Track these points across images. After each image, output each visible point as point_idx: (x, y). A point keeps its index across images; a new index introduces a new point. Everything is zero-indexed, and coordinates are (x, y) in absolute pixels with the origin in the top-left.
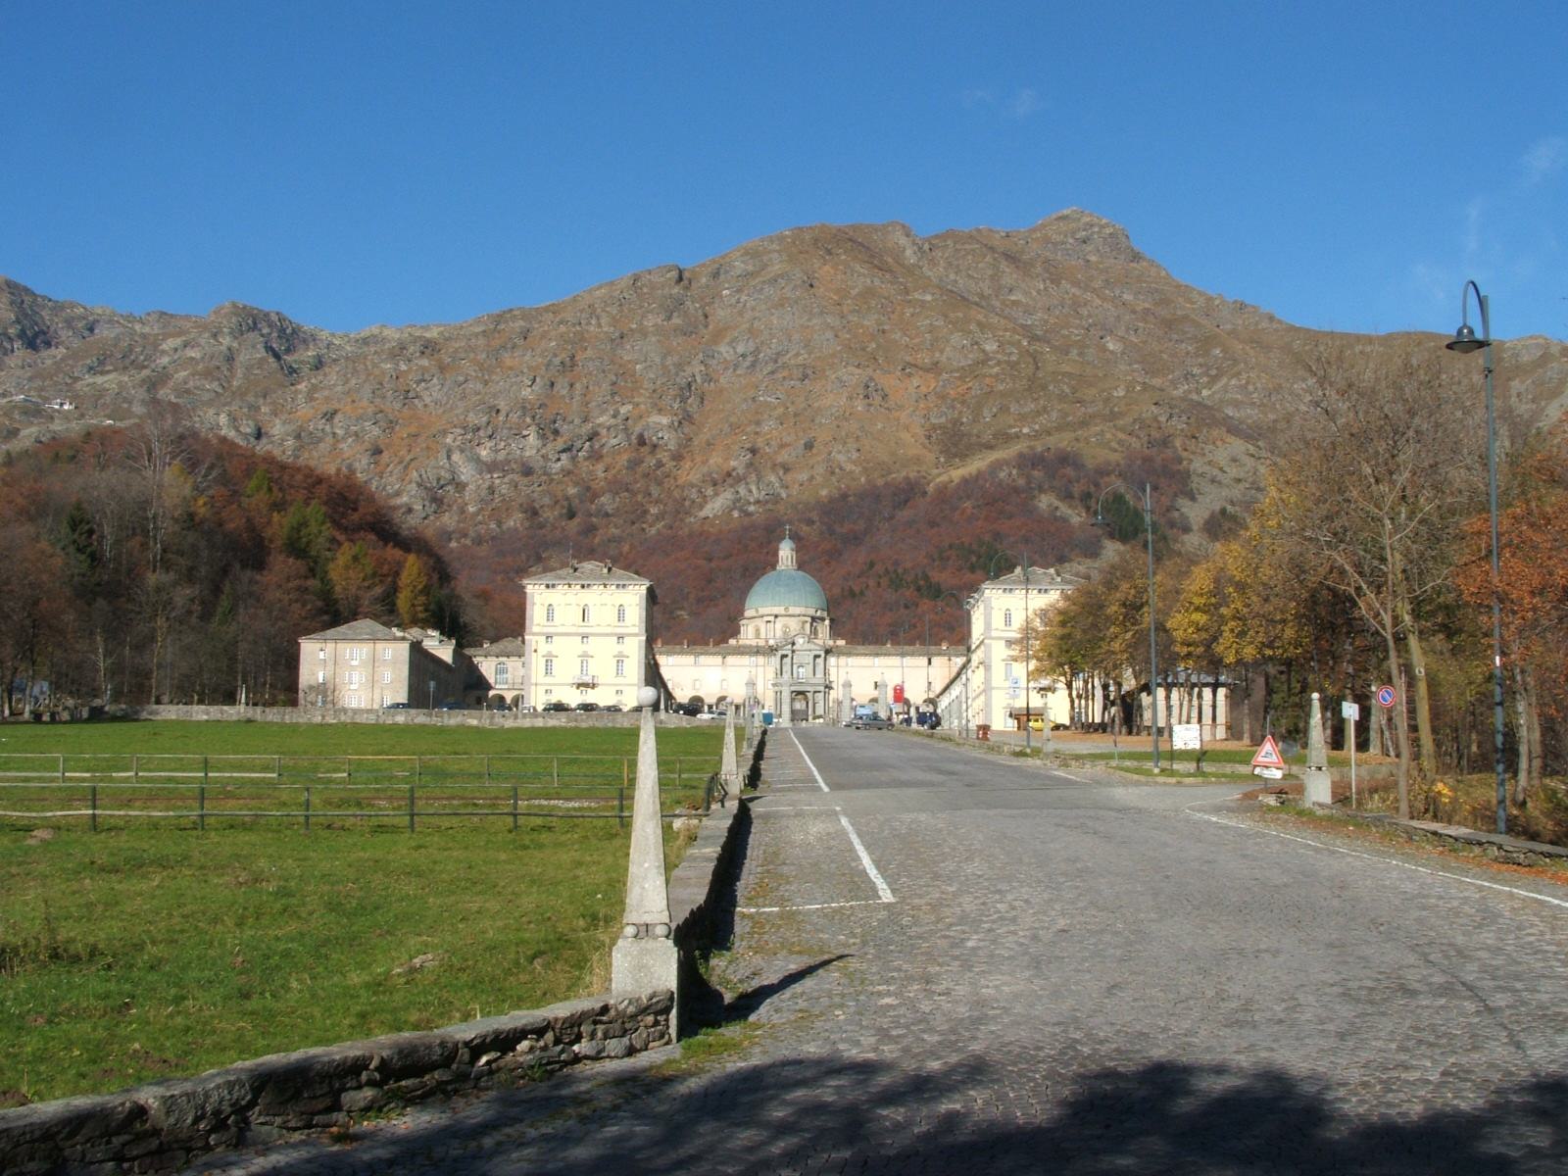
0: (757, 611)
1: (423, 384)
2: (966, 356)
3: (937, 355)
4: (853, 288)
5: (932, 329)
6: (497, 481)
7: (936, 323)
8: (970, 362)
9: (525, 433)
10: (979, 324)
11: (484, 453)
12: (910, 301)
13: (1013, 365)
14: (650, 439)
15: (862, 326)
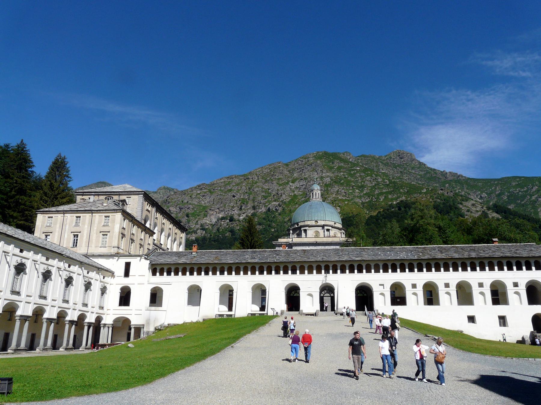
0: (298, 225)
1: (204, 197)
2: (372, 183)
3: (363, 183)
4: (335, 166)
5: (360, 176)
6: (223, 223)
7: (362, 175)
8: (374, 185)
9: (233, 209)
10: (375, 174)
11: (220, 216)
12: (353, 169)
13: (388, 185)
14: (272, 209)
15: (339, 176)
